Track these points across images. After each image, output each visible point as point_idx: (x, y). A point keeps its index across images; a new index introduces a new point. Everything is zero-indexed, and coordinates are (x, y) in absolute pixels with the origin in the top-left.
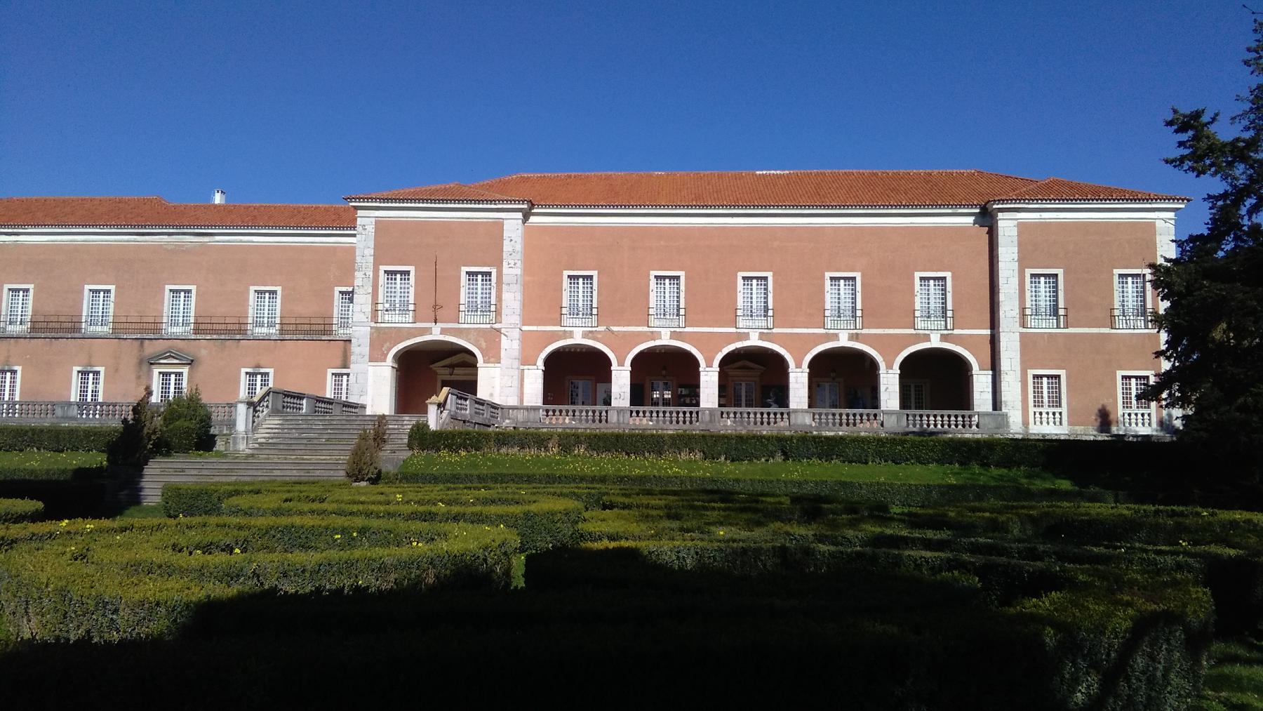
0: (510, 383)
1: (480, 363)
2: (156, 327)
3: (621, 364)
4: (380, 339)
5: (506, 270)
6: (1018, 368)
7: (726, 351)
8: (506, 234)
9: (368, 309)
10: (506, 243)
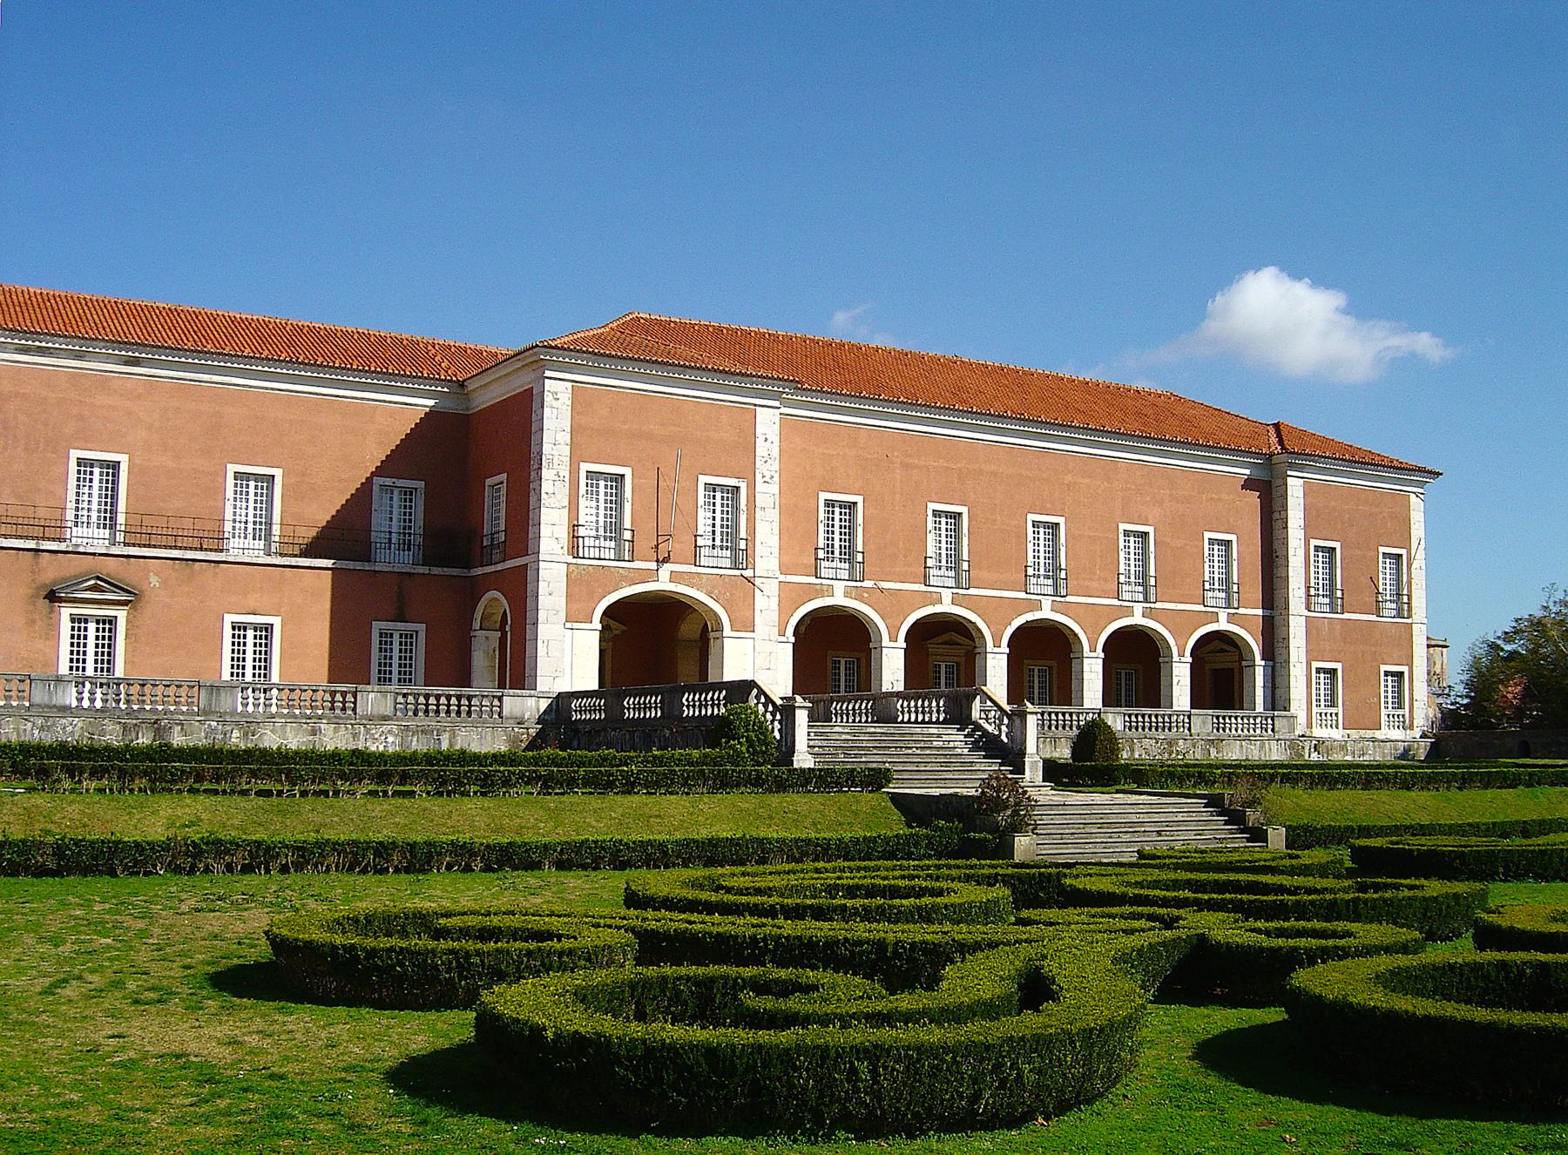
1: (727, 631)
2: (55, 529)
3: (894, 639)
4: (579, 586)
5: (760, 486)
7: (1017, 623)
9: (563, 532)
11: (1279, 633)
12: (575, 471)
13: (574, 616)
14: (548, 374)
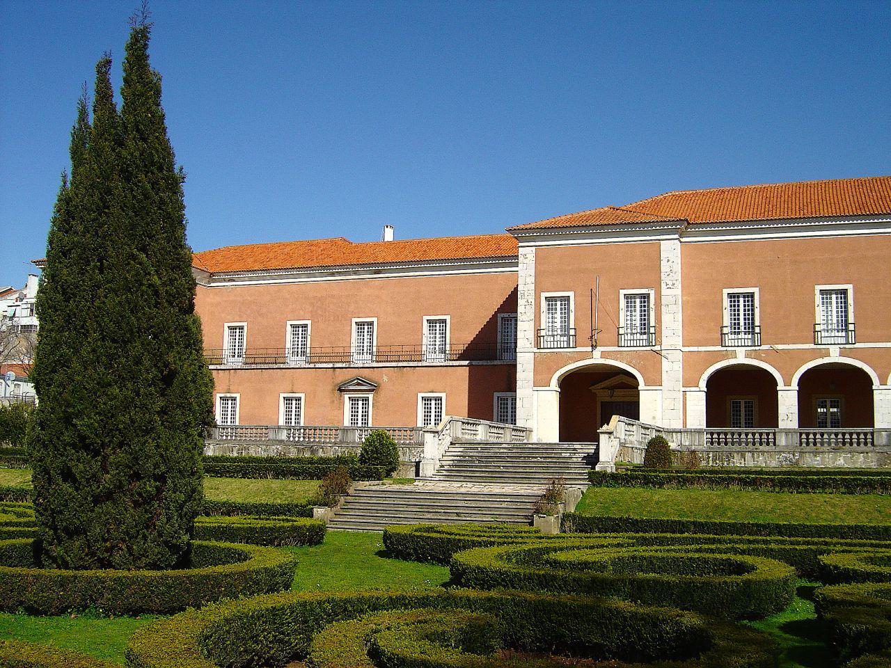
0: (672, 407)
1: (641, 386)
2: (346, 356)
5: (664, 291)
8: (663, 255)
9: (531, 335)
10: (663, 263)
13: (540, 382)
14: (521, 244)
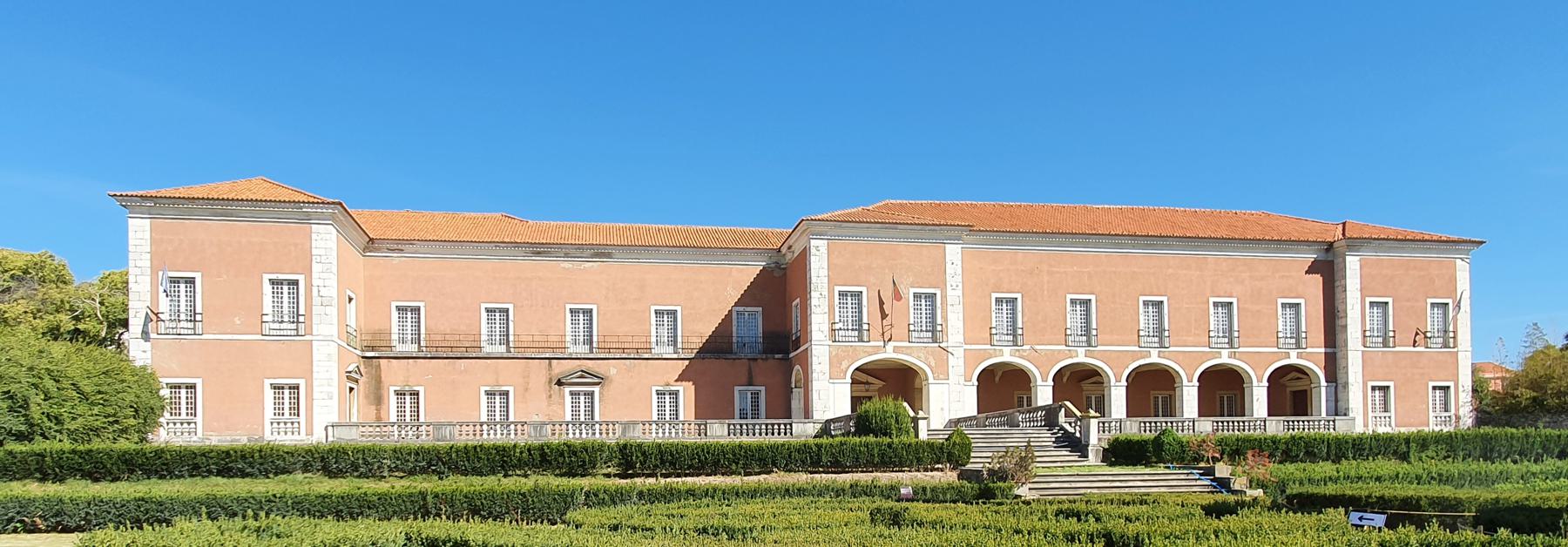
1: (931, 380)
4: (834, 362)
6: (1360, 380)
9: (826, 328)
11: (1340, 363)
12: (831, 291)
